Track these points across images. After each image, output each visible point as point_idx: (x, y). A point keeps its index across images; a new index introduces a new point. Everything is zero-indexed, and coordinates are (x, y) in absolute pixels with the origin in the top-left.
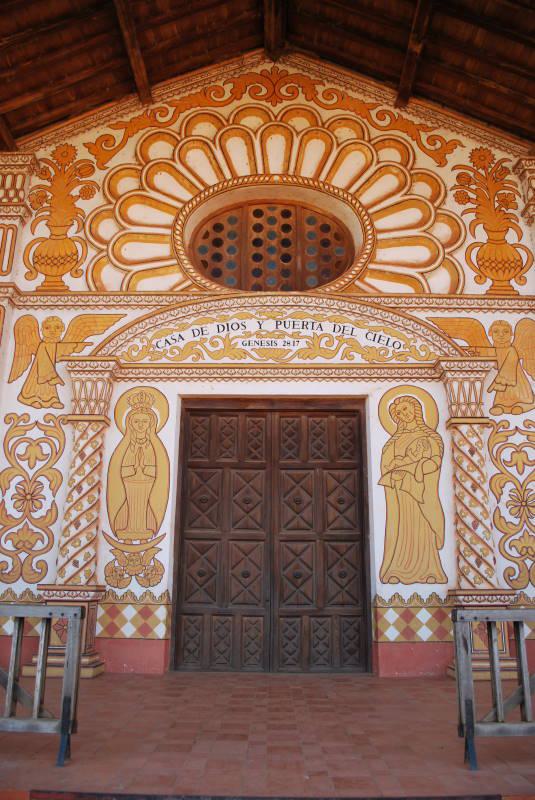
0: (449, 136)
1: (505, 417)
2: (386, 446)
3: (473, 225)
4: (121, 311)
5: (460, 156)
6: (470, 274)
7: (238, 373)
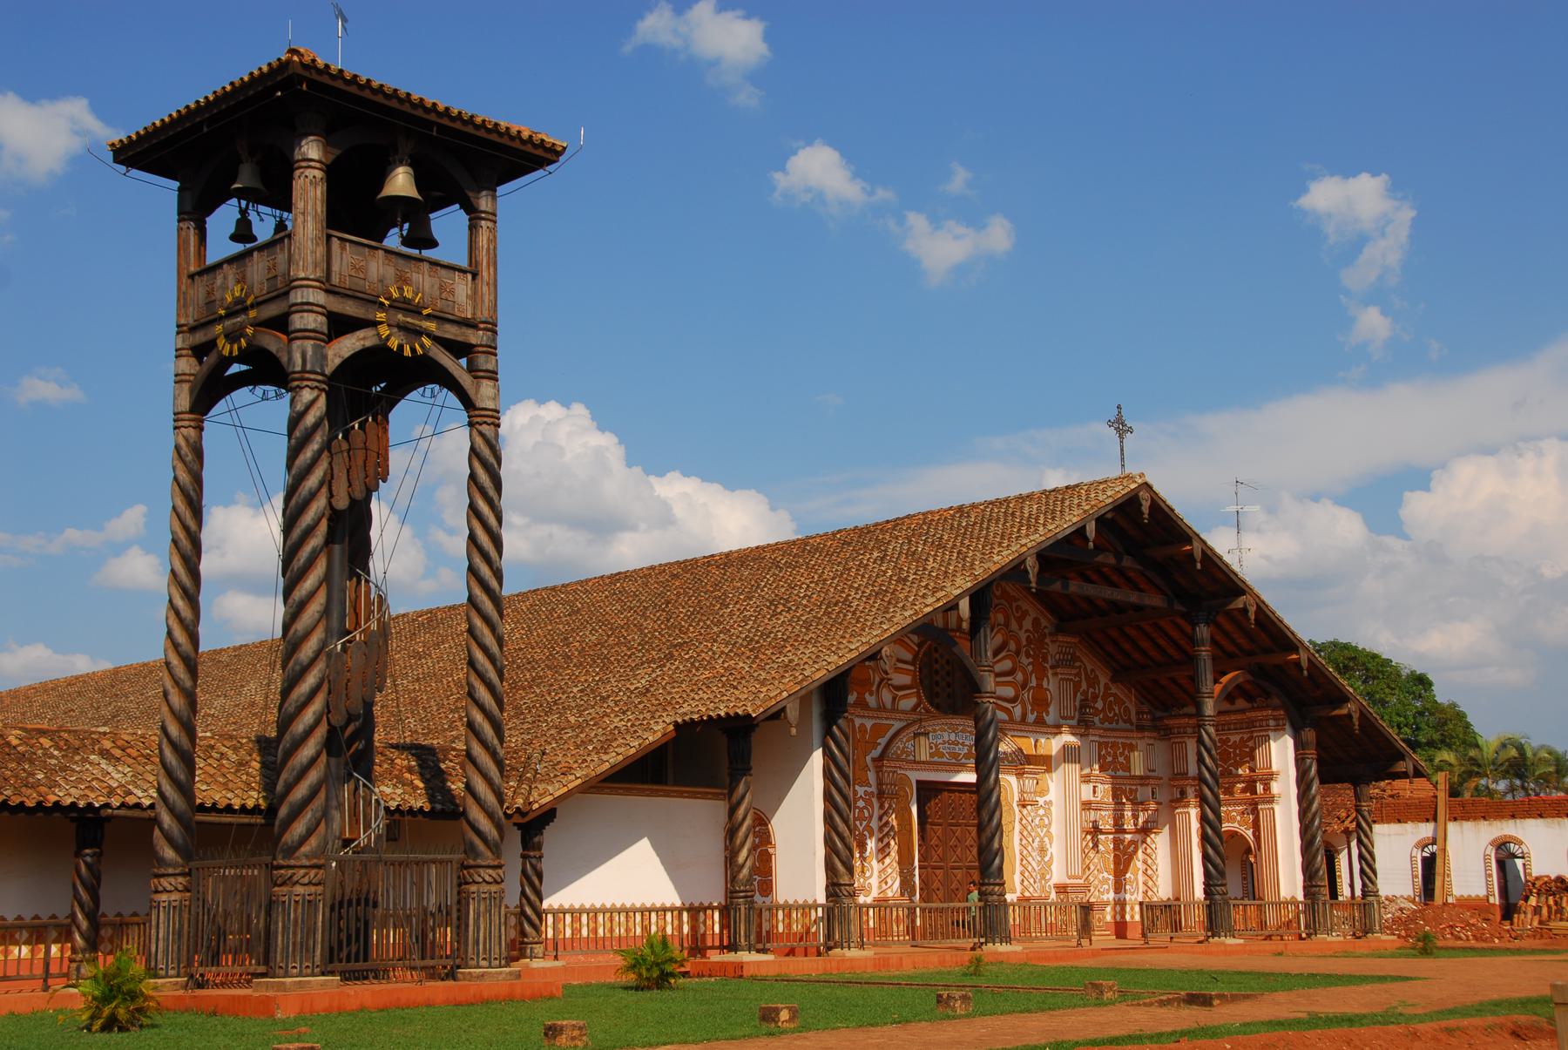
0: (1025, 606)
1: (1038, 799)
3: (1032, 672)
5: (1027, 624)
7: (940, 767)
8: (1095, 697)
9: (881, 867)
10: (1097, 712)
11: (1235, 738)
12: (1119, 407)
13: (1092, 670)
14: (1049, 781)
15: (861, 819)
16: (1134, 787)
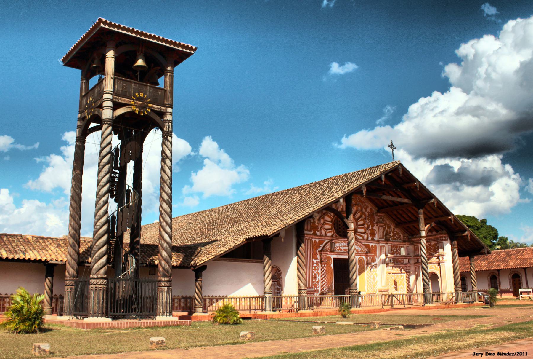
0: (367, 205)
3: (370, 225)
4: (325, 240)
5: (368, 210)
6: (369, 235)
8: (390, 232)
9: (322, 284)
10: (391, 237)
11: (433, 243)
12: (392, 141)
13: (389, 224)
14: (376, 258)
15: (315, 269)
16: (403, 259)
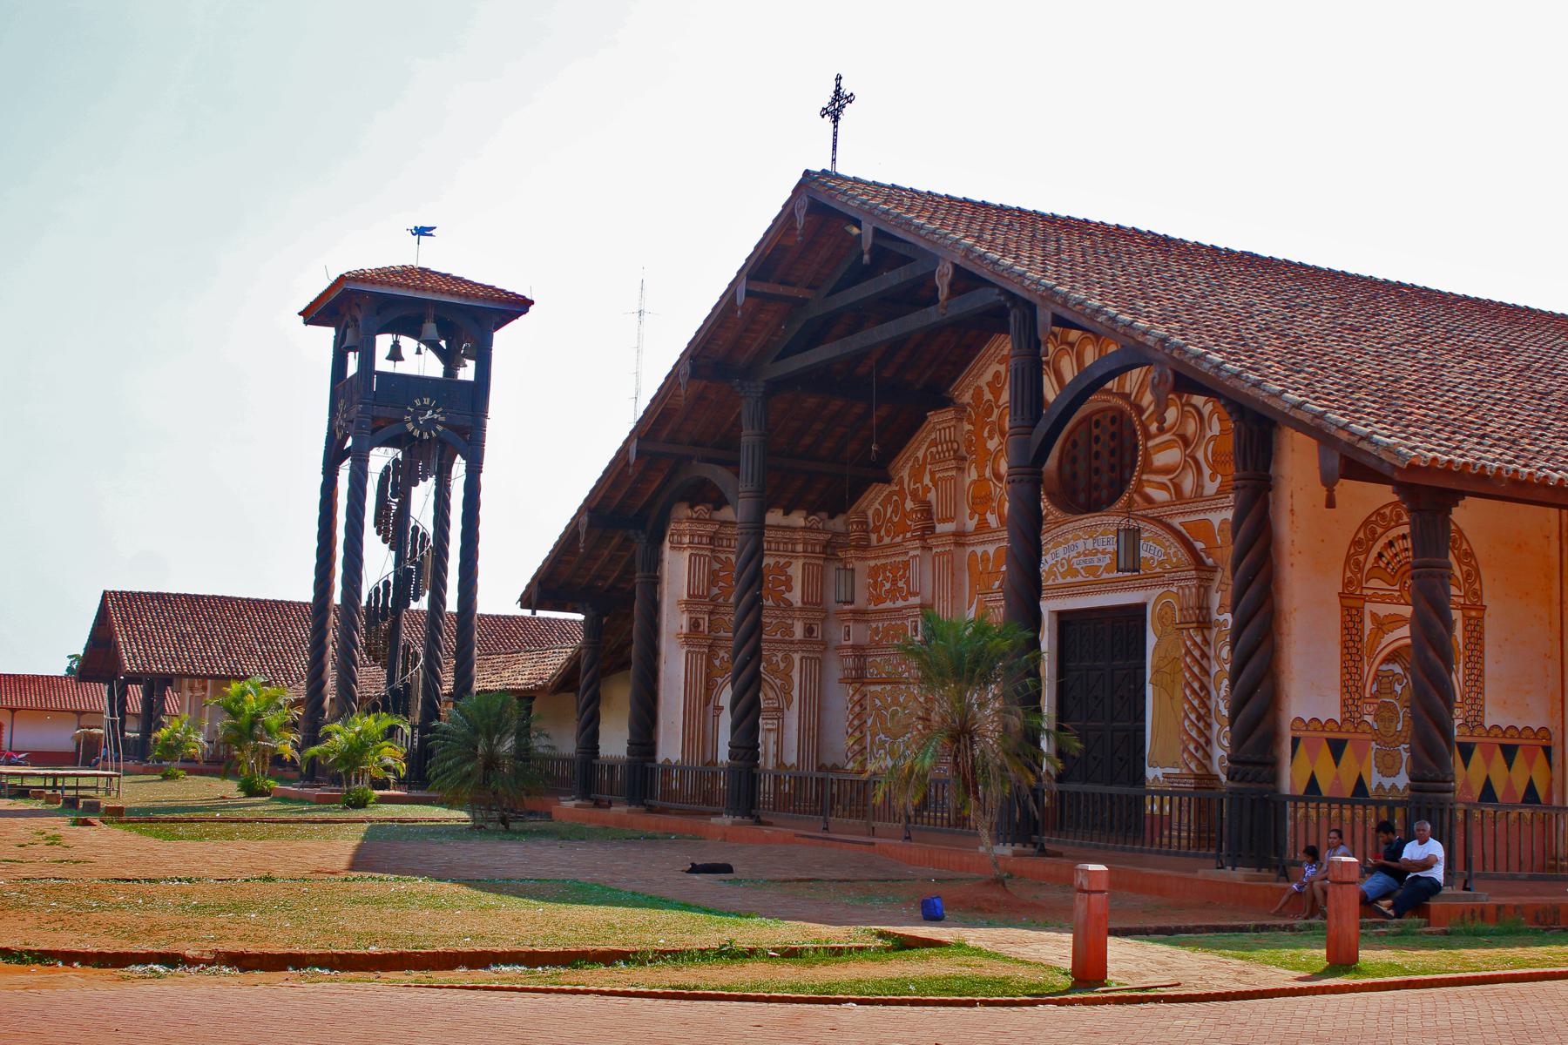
2: (1155, 648)
6: (1207, 471)
